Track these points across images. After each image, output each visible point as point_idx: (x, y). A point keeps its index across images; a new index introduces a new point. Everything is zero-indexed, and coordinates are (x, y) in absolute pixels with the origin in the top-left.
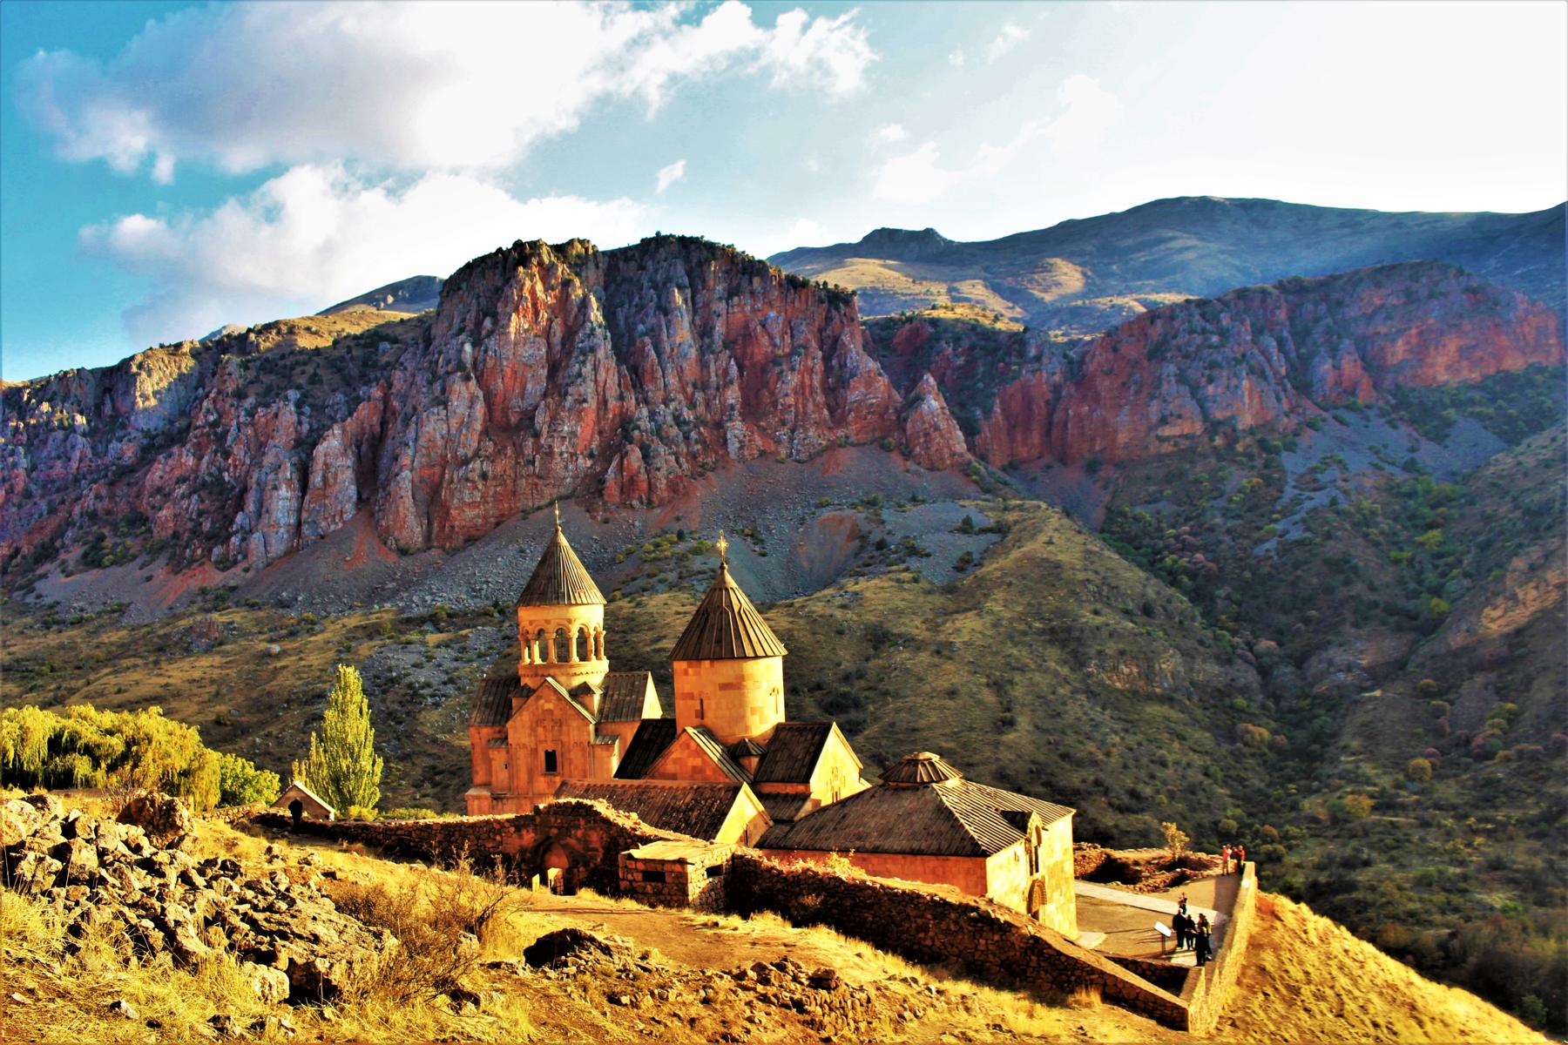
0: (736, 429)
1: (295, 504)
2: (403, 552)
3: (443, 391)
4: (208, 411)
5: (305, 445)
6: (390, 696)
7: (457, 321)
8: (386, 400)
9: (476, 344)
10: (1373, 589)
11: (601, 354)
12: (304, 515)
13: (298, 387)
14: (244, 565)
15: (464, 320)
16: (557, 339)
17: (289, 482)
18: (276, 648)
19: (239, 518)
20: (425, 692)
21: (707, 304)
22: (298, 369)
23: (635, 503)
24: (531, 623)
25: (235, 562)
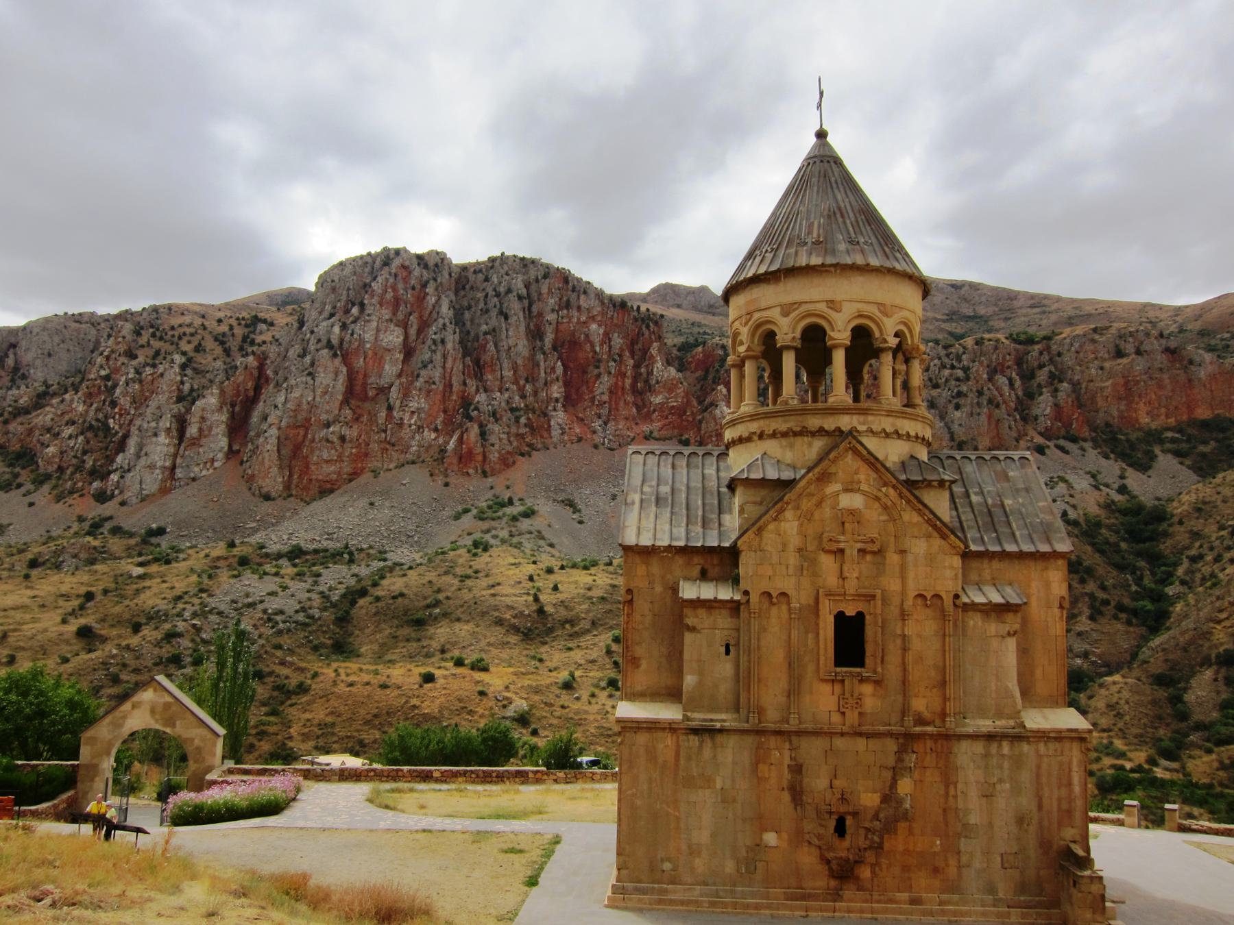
0: (559, 417)
1: (172, 450)
2: (267, 497)
3: (312, 364)
4: (101, 367)
5: (187, 398)
7: (328, 307)
8: (261, 368)
9: (344, 327)
10: (1103, 588)
11: (449, 346)
12: (179, 461)
13: (184, 353)
14: (119, 499)
15: (334, 307)
16: (413, 331)
18: (140, 571)
19: (119, 459)
20: (279, 618)
21: (540, 314)
22: (186, 339)
23: (471, 471)
24: (786, 310)
25: (112, 496)
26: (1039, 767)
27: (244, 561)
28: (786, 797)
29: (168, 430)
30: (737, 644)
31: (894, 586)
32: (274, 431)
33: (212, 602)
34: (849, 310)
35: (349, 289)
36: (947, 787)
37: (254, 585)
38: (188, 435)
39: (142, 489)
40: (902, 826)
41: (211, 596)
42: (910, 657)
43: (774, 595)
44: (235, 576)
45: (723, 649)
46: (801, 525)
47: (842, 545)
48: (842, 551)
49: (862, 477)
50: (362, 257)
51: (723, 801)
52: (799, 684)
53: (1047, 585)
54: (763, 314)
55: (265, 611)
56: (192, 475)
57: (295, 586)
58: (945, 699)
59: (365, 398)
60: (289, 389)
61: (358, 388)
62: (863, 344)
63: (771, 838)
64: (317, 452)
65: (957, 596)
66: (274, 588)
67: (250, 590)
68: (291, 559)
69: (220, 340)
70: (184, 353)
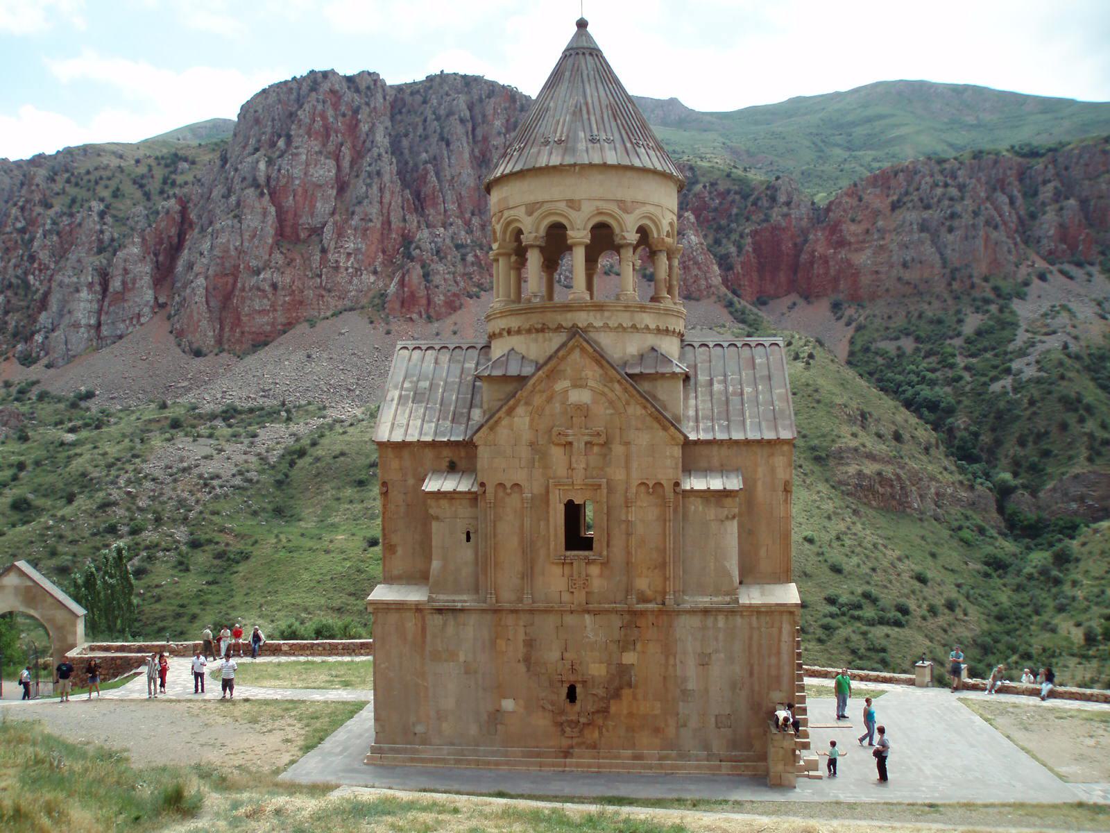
1: (95, 306)
2: (198, 353)
3: (238, 204)
4: (17, 219)
6: (180, 486)
7: (252, 141)
8: (184, 212)
9: (270, 162)
11: (386, 178)
12: (103, 318)
13: (102, 200)
14: (45, 361)
15: (259, 141)
16: (346, 164)
17: (90, 285)
18: (70, 437)
20: (215, 482)
21: (485, 139)
22: (103, 183)
23: (415, 316)
24: (531, 209)
25: (38, 359)
26: (751, 638)
27: (176, 424)
28: (522, 668)
29: (90, 285)
30: (476, 531)
31: (618, 475)
32: (201, 281)
33: (147, 468)
34: (588, 209)
35: (273, 120)
36: (667, 658)
37: (190, 449)
38: (111, 290)
39: (68, 350)
40: (626, 692)
41: (144, 461)
42: (633, 541)
43: (508, 485)
44: (168, 440)
45: (464, 536)
46: (532, 420)
47: (570, 439)
48: (570, 444)
49: (590, 374)
50: (286, 82)
51: (466, 673)
52: (532, 568)
53: (773, 470)
54: (512, 212)
55: (200, 476)
56: (119, 332)
57: (229, 448)
58: (666, 579)
59: (298, 240)
60: (215, 235)
61: (288, 230)
62: (603, 238)
63: (508, 704)
64: (248, 302)
65: (677, 484)
66: (208, 451)
67: (185, 454)
68: (225, 420)
69: (139, 183)
70: (102, 200)
